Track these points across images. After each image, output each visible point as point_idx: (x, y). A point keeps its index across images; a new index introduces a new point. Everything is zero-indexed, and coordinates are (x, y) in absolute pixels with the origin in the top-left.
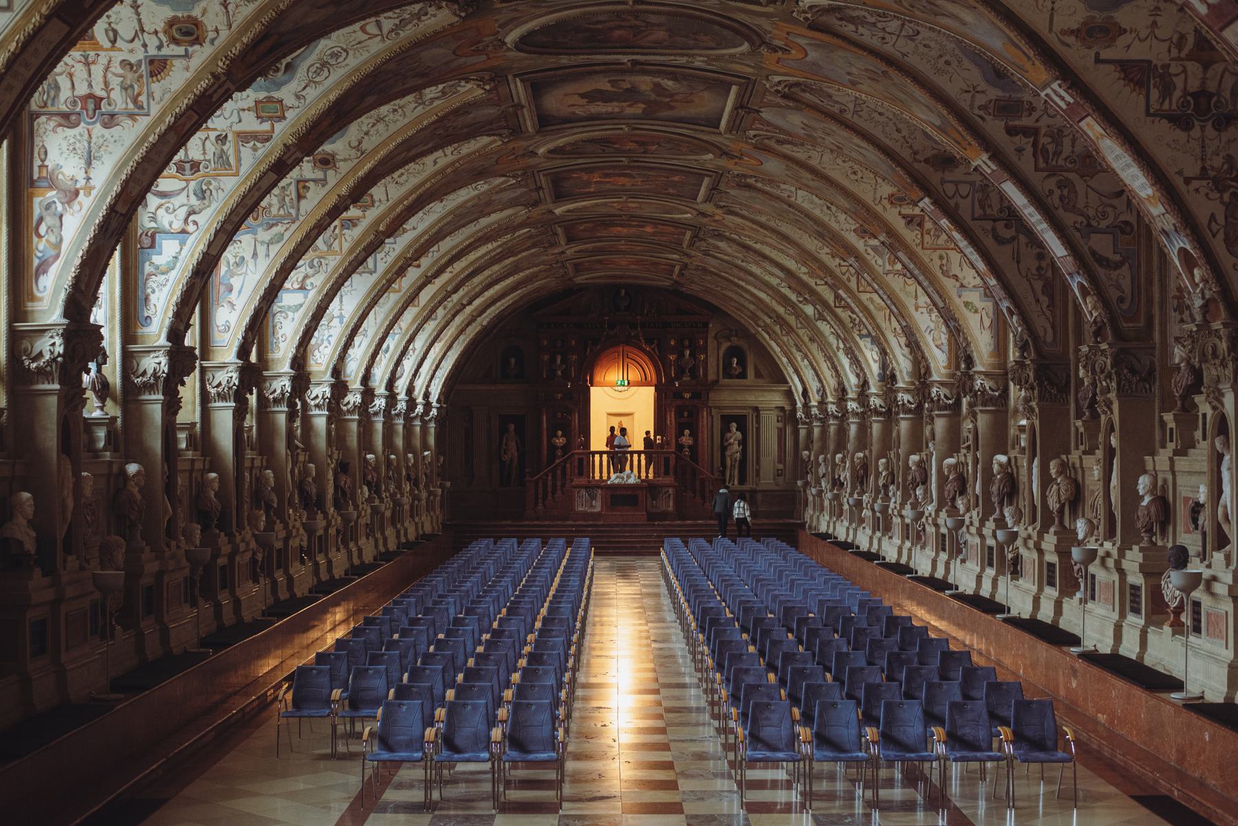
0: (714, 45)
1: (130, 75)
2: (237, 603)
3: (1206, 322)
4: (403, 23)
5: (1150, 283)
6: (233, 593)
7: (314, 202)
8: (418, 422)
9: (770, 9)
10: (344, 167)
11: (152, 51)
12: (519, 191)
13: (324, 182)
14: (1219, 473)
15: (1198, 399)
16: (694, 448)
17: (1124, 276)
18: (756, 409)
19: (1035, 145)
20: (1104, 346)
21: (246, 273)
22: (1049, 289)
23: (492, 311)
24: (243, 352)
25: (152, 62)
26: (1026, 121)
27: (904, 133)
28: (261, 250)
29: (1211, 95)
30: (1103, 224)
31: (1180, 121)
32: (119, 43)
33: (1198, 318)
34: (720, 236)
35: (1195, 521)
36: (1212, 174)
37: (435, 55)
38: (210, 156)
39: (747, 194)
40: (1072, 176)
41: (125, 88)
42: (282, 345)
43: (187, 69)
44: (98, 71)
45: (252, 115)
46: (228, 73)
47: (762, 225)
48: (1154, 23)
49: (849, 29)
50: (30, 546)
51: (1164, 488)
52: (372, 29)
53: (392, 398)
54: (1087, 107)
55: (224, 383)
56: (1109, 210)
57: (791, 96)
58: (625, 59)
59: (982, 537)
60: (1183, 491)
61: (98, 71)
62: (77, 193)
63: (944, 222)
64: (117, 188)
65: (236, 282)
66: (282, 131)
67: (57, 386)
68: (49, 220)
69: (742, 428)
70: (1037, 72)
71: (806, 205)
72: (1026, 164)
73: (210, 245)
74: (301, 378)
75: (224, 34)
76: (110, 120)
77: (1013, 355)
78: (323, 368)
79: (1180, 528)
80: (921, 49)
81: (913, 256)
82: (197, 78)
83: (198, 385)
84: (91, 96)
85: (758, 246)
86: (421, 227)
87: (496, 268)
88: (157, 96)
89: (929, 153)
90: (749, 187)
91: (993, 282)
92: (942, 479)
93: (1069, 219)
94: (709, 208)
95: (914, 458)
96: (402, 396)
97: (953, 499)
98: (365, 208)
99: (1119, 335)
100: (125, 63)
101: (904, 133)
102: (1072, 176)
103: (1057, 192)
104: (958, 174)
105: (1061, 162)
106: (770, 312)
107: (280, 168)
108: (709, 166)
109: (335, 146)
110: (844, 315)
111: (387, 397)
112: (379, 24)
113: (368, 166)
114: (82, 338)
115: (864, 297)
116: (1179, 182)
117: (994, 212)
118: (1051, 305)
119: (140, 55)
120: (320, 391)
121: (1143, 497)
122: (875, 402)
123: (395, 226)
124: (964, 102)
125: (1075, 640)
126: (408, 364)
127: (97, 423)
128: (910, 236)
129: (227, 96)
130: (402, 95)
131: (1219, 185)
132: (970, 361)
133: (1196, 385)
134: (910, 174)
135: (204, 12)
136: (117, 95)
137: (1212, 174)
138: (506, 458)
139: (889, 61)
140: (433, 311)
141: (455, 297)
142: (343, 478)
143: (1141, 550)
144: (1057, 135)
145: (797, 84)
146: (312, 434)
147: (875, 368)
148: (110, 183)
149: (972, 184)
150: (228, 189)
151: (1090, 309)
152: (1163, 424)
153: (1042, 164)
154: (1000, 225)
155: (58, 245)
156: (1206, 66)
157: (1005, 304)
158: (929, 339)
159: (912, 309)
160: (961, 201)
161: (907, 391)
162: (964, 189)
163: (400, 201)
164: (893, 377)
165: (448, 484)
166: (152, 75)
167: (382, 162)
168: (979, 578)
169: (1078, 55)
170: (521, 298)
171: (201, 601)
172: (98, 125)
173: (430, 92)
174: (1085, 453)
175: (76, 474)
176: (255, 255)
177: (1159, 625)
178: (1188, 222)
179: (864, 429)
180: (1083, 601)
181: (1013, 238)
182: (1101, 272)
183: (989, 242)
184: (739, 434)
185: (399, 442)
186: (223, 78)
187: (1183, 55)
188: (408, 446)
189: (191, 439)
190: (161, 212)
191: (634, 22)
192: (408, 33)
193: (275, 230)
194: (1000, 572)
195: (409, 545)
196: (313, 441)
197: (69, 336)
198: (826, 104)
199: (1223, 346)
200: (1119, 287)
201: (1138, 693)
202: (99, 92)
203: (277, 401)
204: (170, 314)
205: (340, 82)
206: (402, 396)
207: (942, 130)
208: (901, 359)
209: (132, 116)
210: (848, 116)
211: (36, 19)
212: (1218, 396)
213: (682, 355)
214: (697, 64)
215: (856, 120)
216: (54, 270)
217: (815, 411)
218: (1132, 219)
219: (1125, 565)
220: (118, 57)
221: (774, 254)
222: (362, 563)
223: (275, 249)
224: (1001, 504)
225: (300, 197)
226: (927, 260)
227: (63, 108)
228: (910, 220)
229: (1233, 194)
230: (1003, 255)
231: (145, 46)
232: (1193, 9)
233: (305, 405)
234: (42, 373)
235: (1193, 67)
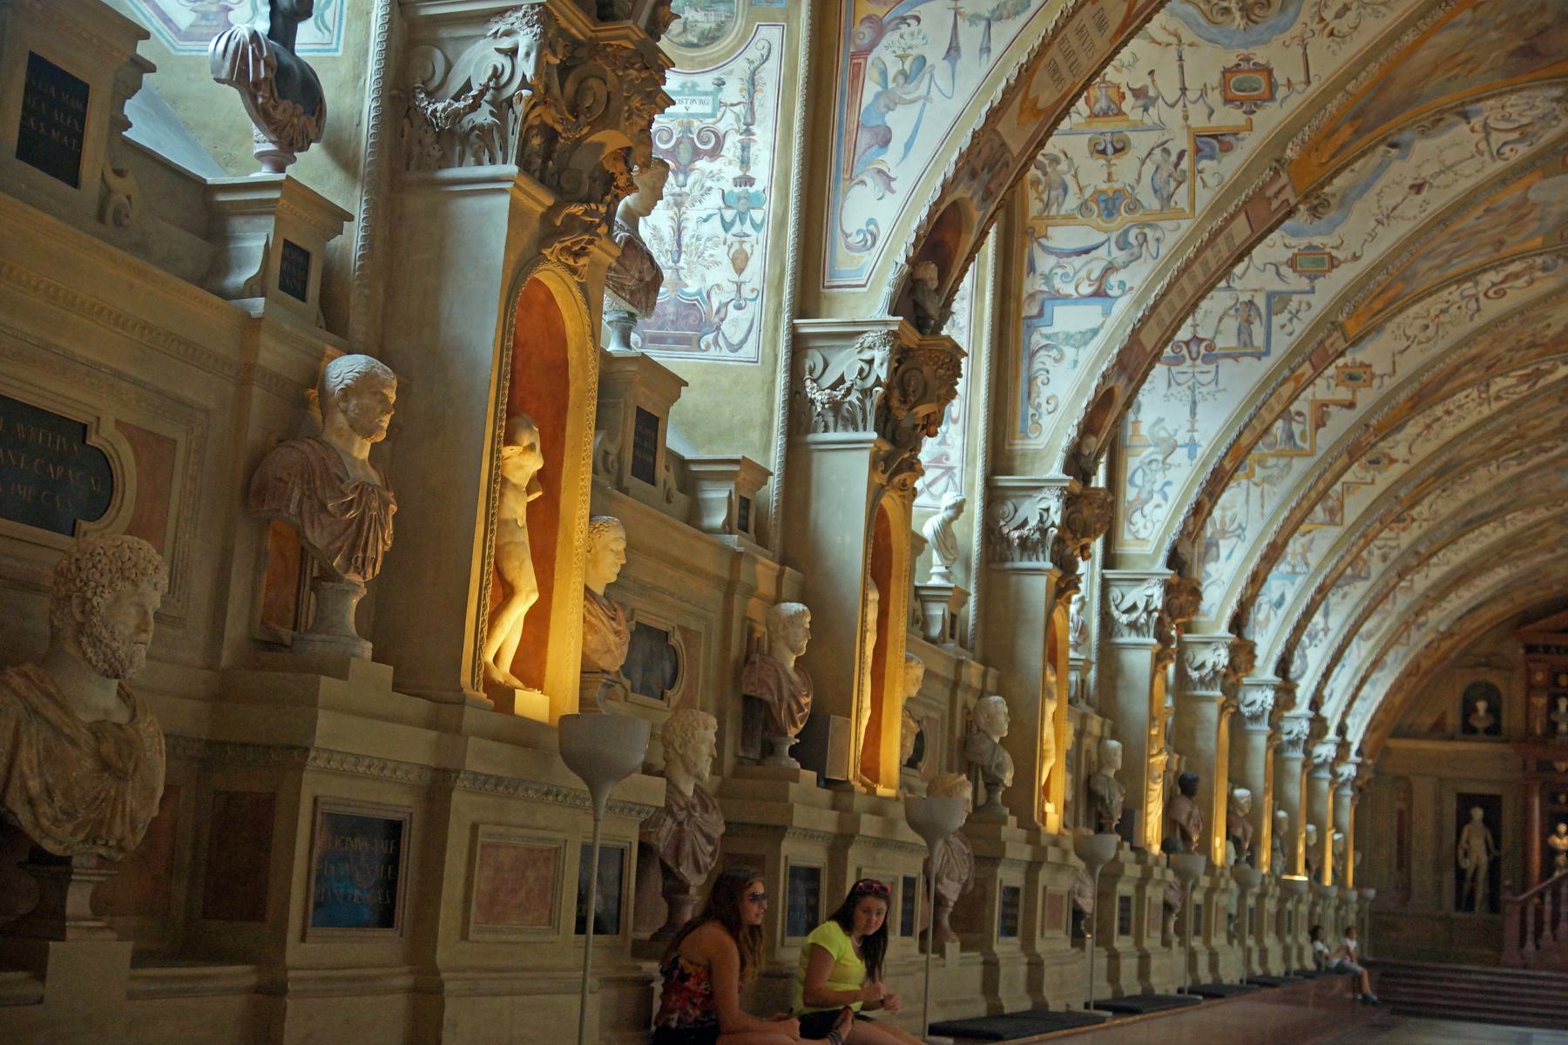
8: (1325, 774)
21: (927, 98)
23: (1457, 602)
28: (971, 37)
42: (1047, 422)
55: (851, 377)
65: (899, 121)
78: (1149, 549)
83: (781, 379)
86: (1371, 255)
111: (1277, 689)
138: (1467, 864)
142: (1184, 806)
146: (1120, 683)
163: (1337, 85)
165: (1371, 893)
170: (1506, 590)
176: (953, 51)
189: (745, 514)
196: (1123, 698)
222: (1217, 980)
223: (1004, 32)
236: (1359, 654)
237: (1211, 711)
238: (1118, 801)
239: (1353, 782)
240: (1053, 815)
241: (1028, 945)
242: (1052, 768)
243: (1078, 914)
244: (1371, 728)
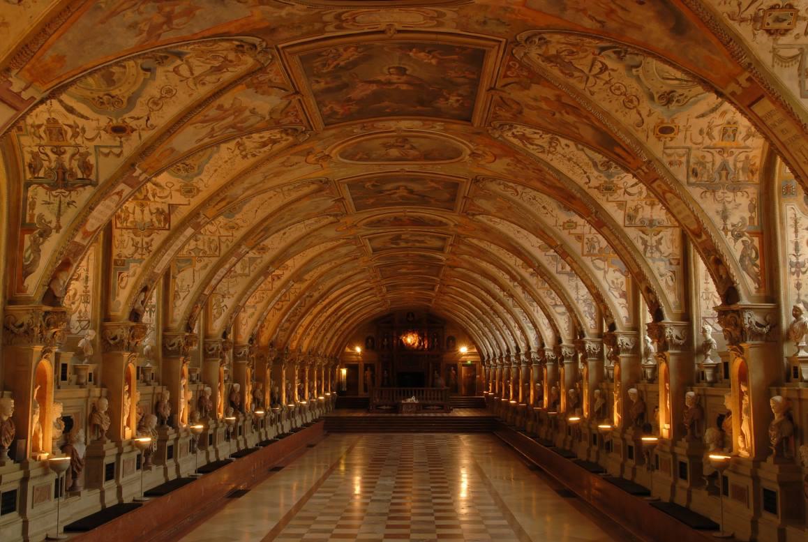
2: (217, 452)
24: (225, 335)
171: (199, 451)
195: (307, 425)
219: (626, 436)
241: (244, 436)
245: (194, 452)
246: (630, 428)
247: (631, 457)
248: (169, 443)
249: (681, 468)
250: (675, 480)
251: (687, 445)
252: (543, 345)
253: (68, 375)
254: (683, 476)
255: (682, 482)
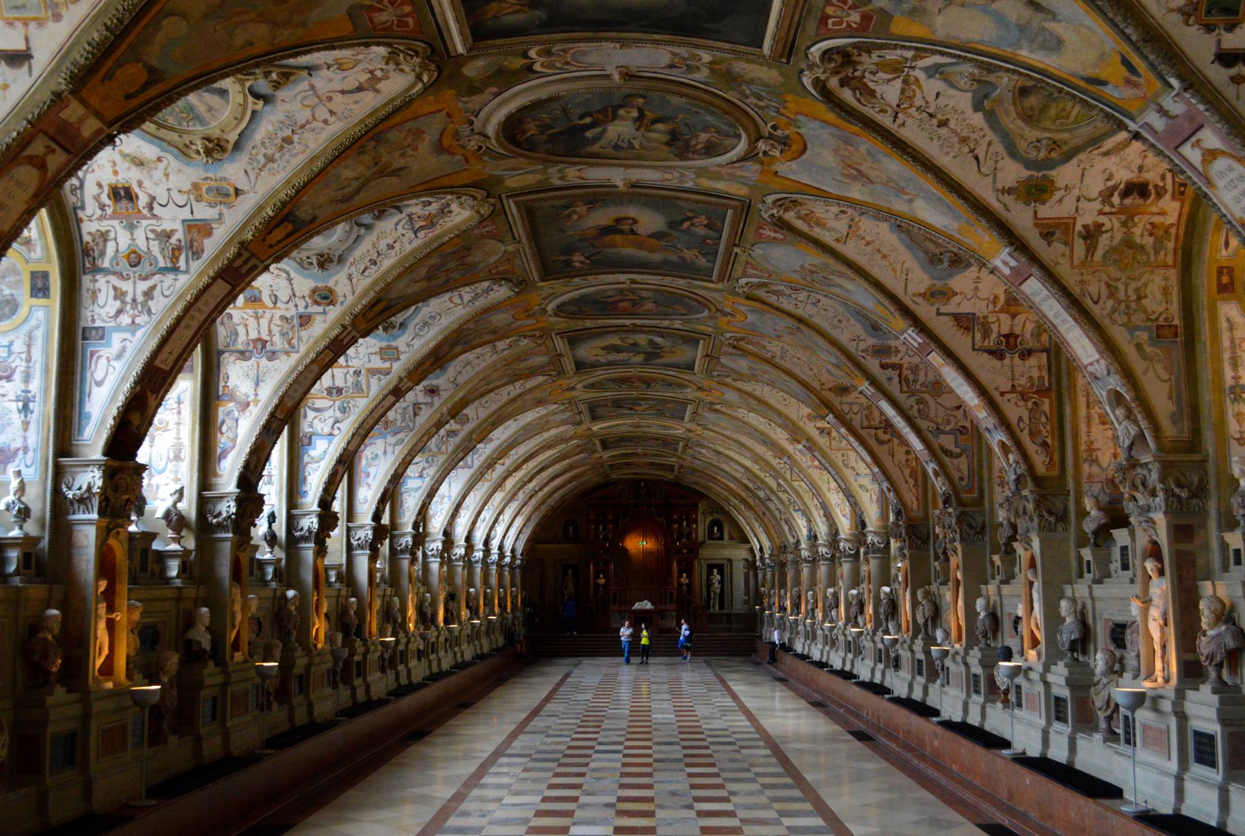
0: (684, 312)
1: (286, 326)
2: (368, 686)
3: (1018, 490)
4: (477, 296)
5: (981, 467)
6: (365, 680)
7: (425, 416)
9: (719, 286)
10: (444, 395)
11: (301, 310)
12: (569, 414)
13: (431, 405)
14: (1031, 595)
15: (1015, 545)
16: (689, 586)
17: (963, 463)
18: (730, 560)
19: (900, 376)
20: (950, 510)
22: (913, 474)
24: (377, 517)
25: (301, 317)
26: (893, 360)
27: (815, 371)
28: (389, 449)
29: (1017, 336)
30: (948, 428)
31: (997, 354)
32: (279, 304)
33: (1013, 487)
34: (702, 446)
35: (1016, 629)
36: (1019, 389)
37: (500, 319)
38: (349, 384)
39: (716, 416)
40: (926, 396)
41: (283, 334)
42: (407, 514)
43: (325, 321)
44: (264, 322)
45: (378, 357)
46: (353, 324)
47: (728, 438)
48: (977, 288)
49: (772, 299)
50: (206, 645)
51: (994, 608)
52: (457, 300)
53: (487, 551)
54: (933, 345)
56: (952, 419)
57: (737, 348)
58: (628, 322)
59: (874, 642)
60: (1007, 609)
61: (264, 322)
62: (248, 404)
63: (843, 430)
64: (276, 401)
65: (372, 470)
66: (398, 368)
67: (231, 535)
68: (229, 423)
69: (721, 572)
70: (899, 322)
71: (755, 423)
72: (894, 388)
73: (348, 444)
74: (420, 537)
75: (350, 298)
76: (272, 356)
77: (892, 518)
79: (1006, 634)
80: (822, 312)
81: (824, 455)
82: (331, 328)
84: (259, 339)
85: (727, 452)
86: (503, 438)
87: (557, 467)
88: (304, 339)
89: (832, 384)
90: (717, 411)
91: (876, 470)
92: (848, 605)
93: (924, 425)
94: (692, 426)
95: (831, 590)
96: (495, 550)
97: (856, 617)
98: (463, 423)
99: (961, 503)
100: (283, 318)
101: (815, 371)
102: (926, 396)
103: (916, 407)
104: (852, 397)
105: (918, 387)
106: (737, 496)
107: (397, 393)
108: (690, 397)
109: (440, 380)
110: (783, 496)
112: (461, 297)
113: (461, 394)
114: (250, 500)
115: (795, 484)
116: (996, 395)
117: (876, 423)
118: (916, 485)
119: (293, 312)
120: (435, 545)
121: (979, 614)
122: (805, 554)
123: (481, 434)
124: (851, 347)
125: (936, 713)
126: (499, 530)
127: (268, 562)
128: (822, 441)
129: (354, 341)
130: (480, 345)
131: (1024, 397)
132: (863, 525)
133: (1013, 538)
134: (820, 399)
135: (336, 283)
136: (277, 339)
137: (1019, 389)
139: (800, 320)
140: (515, 494)
141: (531, 486)
142: (451, 604)
143: (980, 650)
144: (915, 369)
145: (743, 339)
147: (805, 532)
148: (271, 398)
149: (861, 404)
150: (361, 406)
151: (940, 485)
152: (992, 563)
153: (905, 389)
154: (880, 432)
155: (234, 440)
156: (1014, 316)
157: (885, 485)
158: (838, 510)
159: (826, 491)
160: (854, 417)
161: (825, 546)
162: (855, 408)
163: (486, 420)
164: (816, 537)
166: (301, 325)
167: (469, 392)
168: (873, 671)
169: (925, 311)
170: (576, 488)
171: (341, 686)
172: (264, 359)
173: (501, 345)
174: (941, 584)
175: (244, 596)
176: (385, 452)
177: (994, 702)
178: (1004, 422)
179: (798, 573)
180: (943, 686)
181: (889, 440)
182: (947, 460)
183: (873, 443)
184: (719, 577)
185: (494, 580)
186: (350, 328)
187: (997, 309)
188: (501, 585)
189: (339, 577)
190: (316, 422)
191: (631, 297)
192: (482, 302)
193: (399, 436)
194: (887, 667)
195: (498, 650)
197: (240, 501)
198: (763, 353)
199: (1030, 507)
200: (959, 470)
201: (979, 751)
202: (265, 336)
203: (402, 551)
204: (321, 489)
205: (436, 336)
206: (495, 550)
207: (837, 366)
208: (820, 525)
209: (287, 353)
210: (777, 360)
211: (205, 279)
212: (1028, 543)
213: (681, 525)
214: (676, 326)
215: (782, 362)
216: (231, 456)
217: (767, 561)
218: (968, 424)
219: (969, 660)
220: (278, 313)
221: (737, 457)
223: (398, 449)
224: (887, 620)
225: (415, 414)
226: (833, 457)
227: (241, 347)
228: (822, 431)
229: (1035, 403)
230: (882, 452)
231: (296, 306)
232: (1000, 272)
233: (425, 555)
234: (221, 527)
235: (1005, 318)
236: (519, 522)
237: (460, 569)
238: (429, 611)
239: (519, 566)
240: (411, 625)
241: (407, 666)
242: (411, 612)
243: (419, 650)
244: (528, 541)
245: (335, 687)
246: (976, 648)
247: (977, 692)
248: (298, 670)
249: (1057, 705)
250: (1049, 723)
251: (1065, 672)
252: (837, 533)
253: (150, 566)
254: (1061, 718)
255: (1057, 726)
